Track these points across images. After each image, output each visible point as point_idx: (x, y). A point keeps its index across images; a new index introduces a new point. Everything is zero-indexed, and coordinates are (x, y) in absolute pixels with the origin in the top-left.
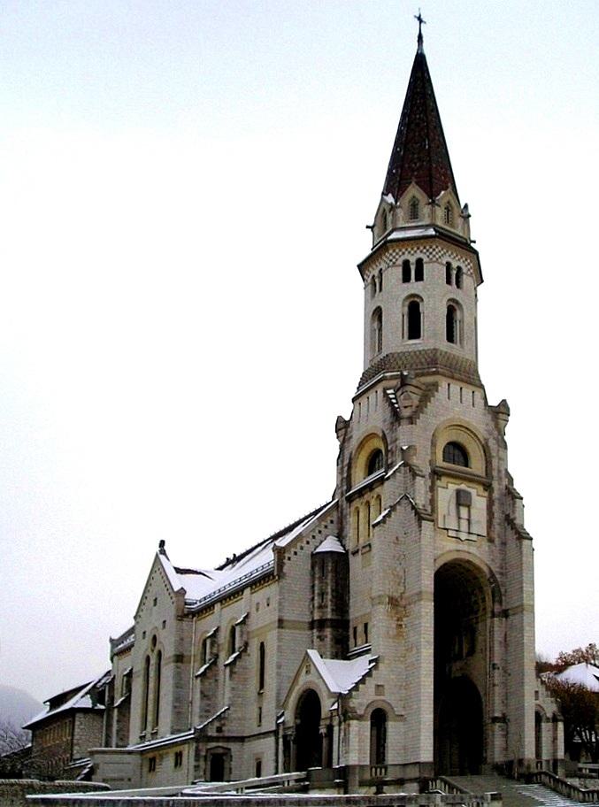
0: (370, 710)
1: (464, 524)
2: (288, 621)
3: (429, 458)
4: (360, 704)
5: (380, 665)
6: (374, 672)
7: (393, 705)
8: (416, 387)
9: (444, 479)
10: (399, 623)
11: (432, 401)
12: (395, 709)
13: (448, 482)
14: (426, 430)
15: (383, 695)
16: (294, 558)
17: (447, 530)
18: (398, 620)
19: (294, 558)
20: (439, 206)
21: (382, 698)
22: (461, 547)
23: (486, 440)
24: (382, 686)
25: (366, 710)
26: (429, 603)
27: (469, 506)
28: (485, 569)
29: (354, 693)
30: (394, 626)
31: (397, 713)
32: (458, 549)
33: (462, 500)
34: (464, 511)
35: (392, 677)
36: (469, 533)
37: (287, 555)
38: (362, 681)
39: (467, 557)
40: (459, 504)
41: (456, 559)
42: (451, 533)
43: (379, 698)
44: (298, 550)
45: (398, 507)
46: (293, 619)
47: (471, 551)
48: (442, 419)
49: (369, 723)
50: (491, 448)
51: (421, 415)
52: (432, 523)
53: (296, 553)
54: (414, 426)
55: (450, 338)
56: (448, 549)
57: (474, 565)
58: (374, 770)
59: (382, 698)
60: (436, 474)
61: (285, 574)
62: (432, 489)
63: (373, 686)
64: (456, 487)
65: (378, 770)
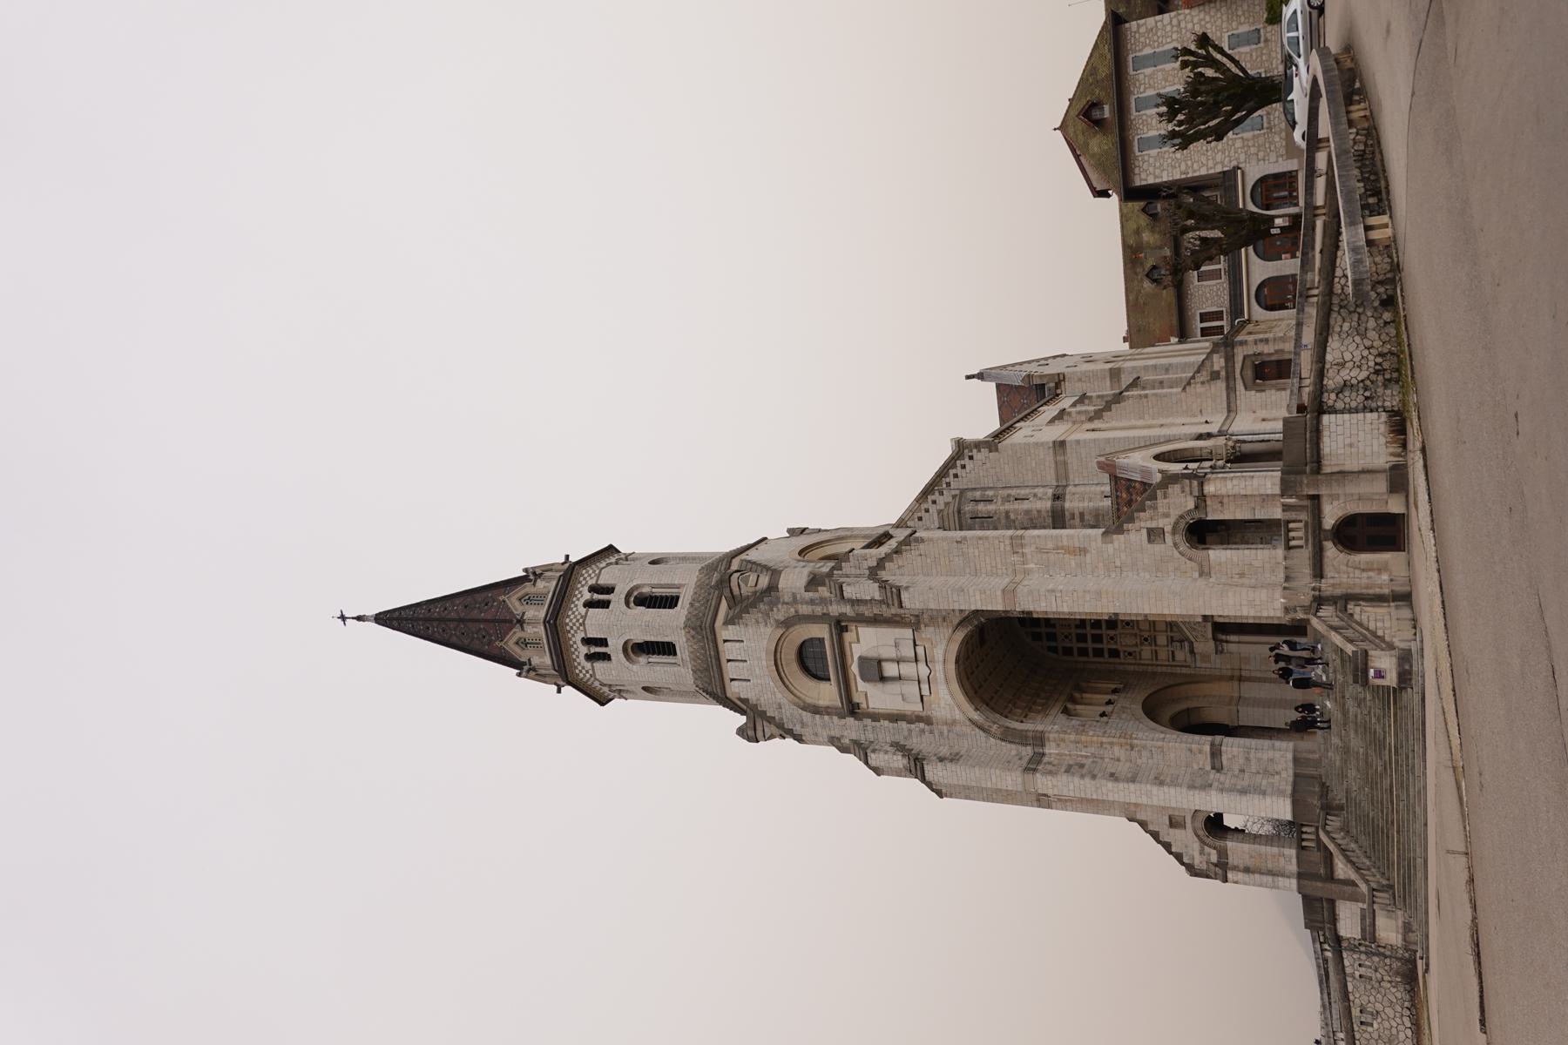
0: (1209, 840)
1: (908, 669)
4: (1202, 853)
6: (1151, 828)
8: (755, 730)
9: (857, 698)
11: (763, 709)
13: (857, 691)
14: (803, 725)
17: (922, 697)
20: (529, 660)
21: (1188, 820)
22: (939, 673)
23: (780, 624)
24: (1170, 818)
25: (1210, 847)
26: (1039, 781)
27: (879, 662)
28: (960, 635)
33: (874, 670)
34: (890, 670)
38: (1167, 847)
39: (952, 666)
40: (883, 679)
43: (1189, 825)
47: (941, 659)
48: (779, 695)
55: (670, 602)
56: (948, 697)
57: (959, 651)
58: (1304, 844)
59: (1188, 820)
60: (852, 709)
62: (875, 717)
65: (1304, 836)
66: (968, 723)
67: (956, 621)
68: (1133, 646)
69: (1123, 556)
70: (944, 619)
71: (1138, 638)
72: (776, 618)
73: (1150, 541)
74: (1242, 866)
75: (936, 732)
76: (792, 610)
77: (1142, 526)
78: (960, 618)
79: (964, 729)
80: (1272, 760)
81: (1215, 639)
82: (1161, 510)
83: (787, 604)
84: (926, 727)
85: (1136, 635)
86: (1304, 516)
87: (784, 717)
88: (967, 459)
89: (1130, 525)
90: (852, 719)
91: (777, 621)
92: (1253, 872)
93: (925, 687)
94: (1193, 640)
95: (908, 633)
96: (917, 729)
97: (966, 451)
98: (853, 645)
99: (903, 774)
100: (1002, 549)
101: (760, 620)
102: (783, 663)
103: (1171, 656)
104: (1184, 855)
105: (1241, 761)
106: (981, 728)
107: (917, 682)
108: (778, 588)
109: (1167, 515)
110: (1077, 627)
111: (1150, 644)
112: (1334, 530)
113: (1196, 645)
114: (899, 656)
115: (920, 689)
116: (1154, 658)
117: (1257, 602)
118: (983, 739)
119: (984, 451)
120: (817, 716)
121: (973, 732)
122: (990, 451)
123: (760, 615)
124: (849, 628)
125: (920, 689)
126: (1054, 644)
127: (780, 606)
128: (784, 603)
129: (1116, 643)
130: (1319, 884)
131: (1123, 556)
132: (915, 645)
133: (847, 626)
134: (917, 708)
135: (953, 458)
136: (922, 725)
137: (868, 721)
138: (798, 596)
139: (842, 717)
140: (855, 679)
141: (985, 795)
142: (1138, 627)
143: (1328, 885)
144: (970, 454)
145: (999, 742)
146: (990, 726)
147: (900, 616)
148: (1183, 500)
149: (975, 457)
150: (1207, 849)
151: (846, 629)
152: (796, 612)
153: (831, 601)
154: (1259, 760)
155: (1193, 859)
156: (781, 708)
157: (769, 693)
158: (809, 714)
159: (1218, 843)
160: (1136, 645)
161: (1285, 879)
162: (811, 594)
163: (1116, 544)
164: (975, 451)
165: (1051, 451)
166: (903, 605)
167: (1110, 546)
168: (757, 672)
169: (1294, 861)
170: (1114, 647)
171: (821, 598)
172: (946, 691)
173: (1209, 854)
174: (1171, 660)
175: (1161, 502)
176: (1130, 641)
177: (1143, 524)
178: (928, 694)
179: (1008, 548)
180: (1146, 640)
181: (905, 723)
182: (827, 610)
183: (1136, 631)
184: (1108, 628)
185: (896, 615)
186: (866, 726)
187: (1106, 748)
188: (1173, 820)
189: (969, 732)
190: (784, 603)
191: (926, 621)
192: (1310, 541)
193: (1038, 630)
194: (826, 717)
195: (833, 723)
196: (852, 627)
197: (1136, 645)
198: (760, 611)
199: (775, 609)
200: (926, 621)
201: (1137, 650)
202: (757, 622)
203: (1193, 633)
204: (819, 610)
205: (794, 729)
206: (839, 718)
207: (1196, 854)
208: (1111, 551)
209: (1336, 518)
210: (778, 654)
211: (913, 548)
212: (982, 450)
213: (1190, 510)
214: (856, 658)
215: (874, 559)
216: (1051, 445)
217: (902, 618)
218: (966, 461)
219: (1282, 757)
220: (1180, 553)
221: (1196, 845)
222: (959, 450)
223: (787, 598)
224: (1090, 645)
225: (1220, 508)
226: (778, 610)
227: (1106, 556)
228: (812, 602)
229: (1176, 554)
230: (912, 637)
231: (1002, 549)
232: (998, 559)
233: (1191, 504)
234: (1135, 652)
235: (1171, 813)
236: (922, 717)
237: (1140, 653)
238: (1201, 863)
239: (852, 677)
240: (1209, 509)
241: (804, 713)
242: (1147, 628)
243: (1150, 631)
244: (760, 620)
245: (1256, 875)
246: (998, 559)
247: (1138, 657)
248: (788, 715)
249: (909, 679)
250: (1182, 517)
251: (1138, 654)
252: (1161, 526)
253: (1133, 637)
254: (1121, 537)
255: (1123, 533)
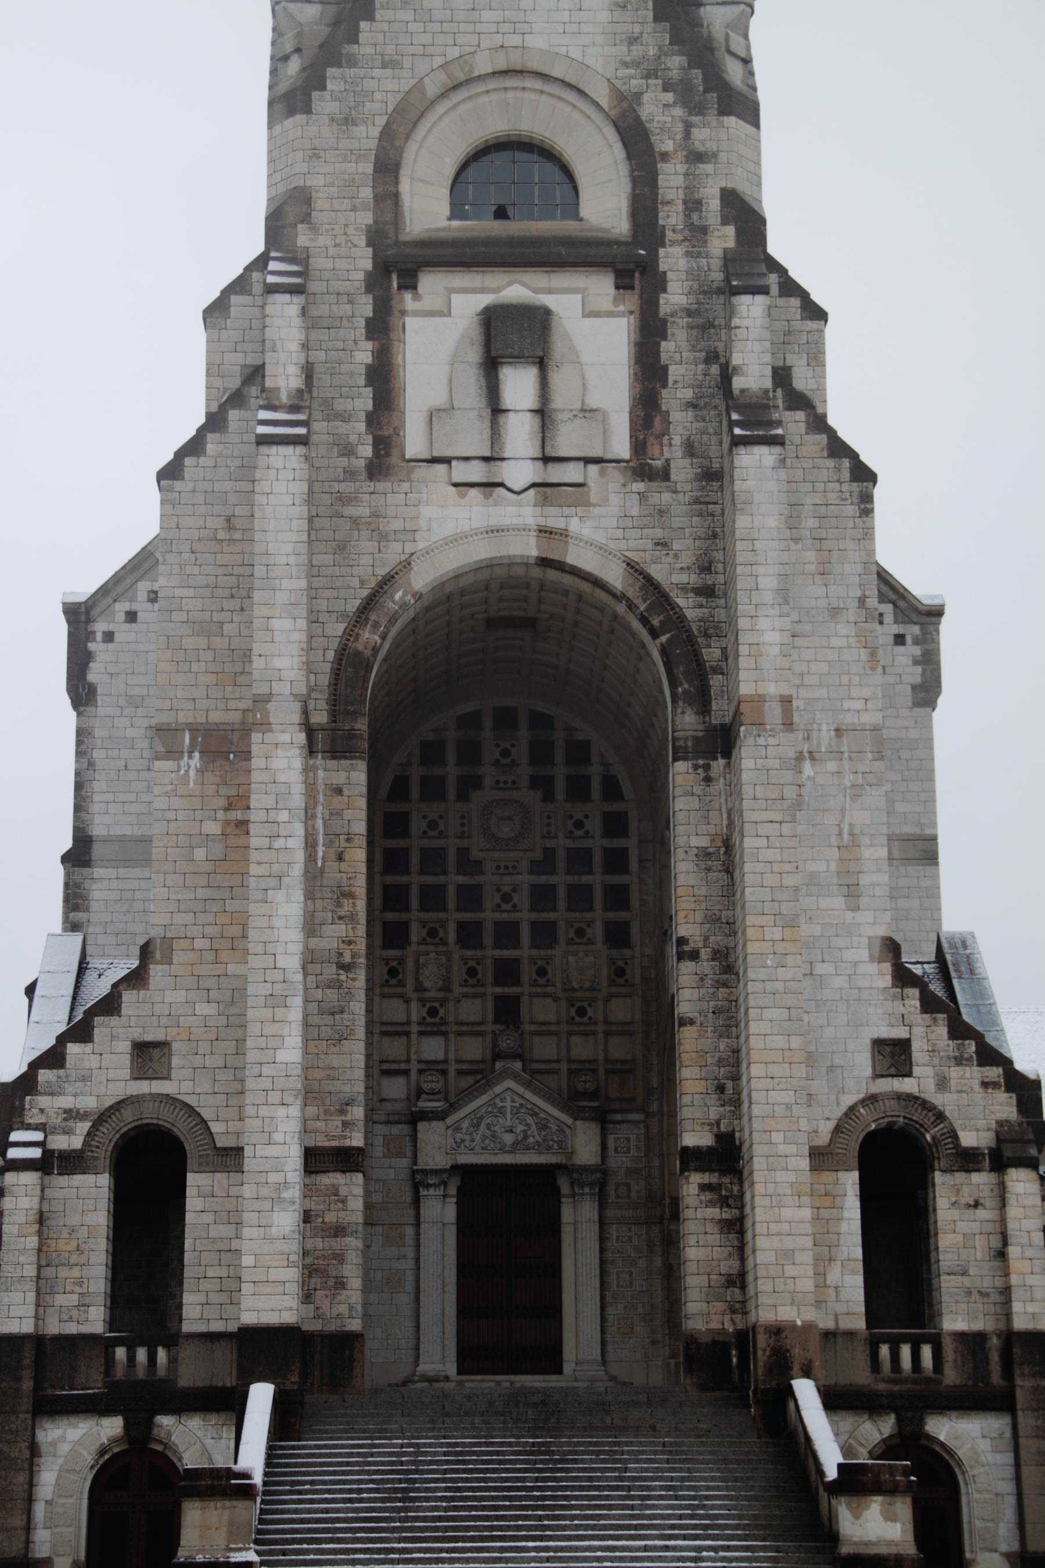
0: (109, 1136)
2: (108, 840)
3: (367, 218)
4: (72, 1115)
5: (157, 972)
6: (128, 997)
7: (206, 1114)
9: (431, 283)
10: (237, 815)
12: (215, 1128)
13: (451, 291)
14: (348, 121)
15: (168, 1078)
16: (124, 632)
17: (447, 461)
18: (226, 809)
19: (124, 632)
24: (163, 1046)
27: (542, 364)
29: (45, 1075)
30: (213, 828)
31: (219, 1145)
32: (494, 522)
35: (203, 1009)
36: (546, 459)
37: (100, 627)
41: (490, 565)
42: (463, 472)
43: (144, 1087)
44: (141, 604)
45: (233, 415)
46: (116, 831)
49: (104, 1180)
50: (653, 127)
51: (331, 72)
52: (300, 450)
53: (132, 617)
54: (300, 118)
56: (449, 529)
61: (92, 690)
63: (125, 1046)
64: (486, 300)
66: (382, 572)
67: (658, 572)
68: (417, 979)
69: (839, 982)
70: (662, 544)
71: (440, 995)
72: (646, 97)
73: (879, 1044)
74: (45, 1208)
75: (347, 487)
76: (669, 146)
77: (915, 1030)
78: (666, 586)
79: (366, 560)
80: (341, 1284)
81: (455, 1168)
82: (954, 1073)
83: (687, 134)
84: (362, 463)
85: (446, 989)
86: (951, 1376)
87: (361, 72)
88: (896, 629)
89: (918, 1004)
90: (368, 264)
91: (638, 96)
92: (40, 1233)
93: (475, 472)
94: (450, 1121)
95: (621, 447)
96: (353, 438)
97: (916, 630)
98: (578, 297)
99: (218, 382)
100: (847, 704)
101: (637, 50)
102: (511, 95)
103: (394, 1066)
104: (61, 1072)
105: (331, 1217)
106: (369, 604)
107: (488, 454)
108: (729, 114)
109: (942, 1084)
110: (463, 853)
111: (422, 1022)
112: (923, 1442)
113: (438, 1125)
114: (560, 416)
115: (467, 459)
116: (385, 1028)
117: (790, 1270)
118: (339, 606)
119: (915, 675)
120: (369, 168)
121: (356, 583)
122: (914, 688)
123: (652, 51)
124: (629, 292)
125: (467, 459)
126: (415, 793)
127: (678, 111)
128: (688, 127)
129: (423, 942)
130: (27, 1385)
131: (839, 982)
132: (588, 461)
133: (632, 288)
134: (415, 443)
135: (902, 597)
136: (367, 451)
137: (366, 307)
138: (709, 168)
139: (376, 238)
140: (483, 290)
141: (179, 592)
142: (465, 996)
143: (26, 1403)
144: (909, 639)
145: (335, 644)
146: (376, 625)
147: (666, 432)
148: (982, 1123)
149: (900, 649)
150: (84, 1127)
151: (623, 283)
152: (665, 156)
153: (699, 255)
154: (340, 1258)
155: (52, 1094)
156: (384, 66)
157: (427, 39)
158: (373, 144)
159: (104, 1153)
160: (420, 988)
161: (32, 1307)
162: (714, 204)
163: (873, 968)
164: (917, 651)
165: (910, 829)
166: (742, 450)
167: (864, 954)
168: (486, 15)
169: (72, 1329)
170: (414, 937)
171: (704, 230)
172: (465, 526)
173: (68, 1132)
174: (385, 1066)
175: (974, 1074)
176: (431, 975)
177: (918, 1032)
178: (456, 479)
179: (850, 719)
180: (433, 1012)
181: (370, 407)
182: (673, 243)
183: (457, 990)
184: (461, 926)
185: (666, 416)
186: (350, 302)
187: (339, 905)
188: (156, 1053)
189: (356, 571)
190: (688, 127)
191: (655, 499)
192: (896, 1388)
193: (451, 756)
194: (367, 193)
195: (354, 209)
196: (632, 300)
197: (420, 988)
198: (662, 53)
199: (670, 97)
200: (655, 499)
201: (409, 990)
202: (633, 40)
203: (466, 1124)
204: (671, 218)
205: (326, 94)
206: (369, 229)
207: (65, 1102)
208: (850, 955)
209: (951, 1444)
210: (536, 84)
211: (845, 487)
212: (919, 669)
213: (956, 1137)
214: (548, 300)
215: (812, 385)
216: (928, 831)
217: (660, 436)
218: (892, 628)
219: (351, 1308)
220: (852, 1109)
221: (90, 1103)
222: (919, 612)
223: (702, 136)
224: (415, 880)
225: (963, 1201)
226: (666, 106)
227: (839, 942)
228: (693, 205)
229: (848, 1100)
230: (609, 456)
231: (847, 704)
232: (822, 693)
233: (968, 1139)
234: (401, 984)
235: (175, 1046)
236: (388, 454)
237: (401, 996)
238: (42, 1111)
239: (493, 278)
240: (960, 1177)
241: (375, 132)
242: (463, 1018)
243: (532, 1023)
244: (637, 50)
245: (36, 1239)
246: (822, 693)
247: (387, 990)
248: (369, 85)
249: (496, 434)
250: (940, 1117)
251: (398, 990)
252: (916, 1071)
253: (441, 983)
254: (887, 980)
255: (894, 986)
